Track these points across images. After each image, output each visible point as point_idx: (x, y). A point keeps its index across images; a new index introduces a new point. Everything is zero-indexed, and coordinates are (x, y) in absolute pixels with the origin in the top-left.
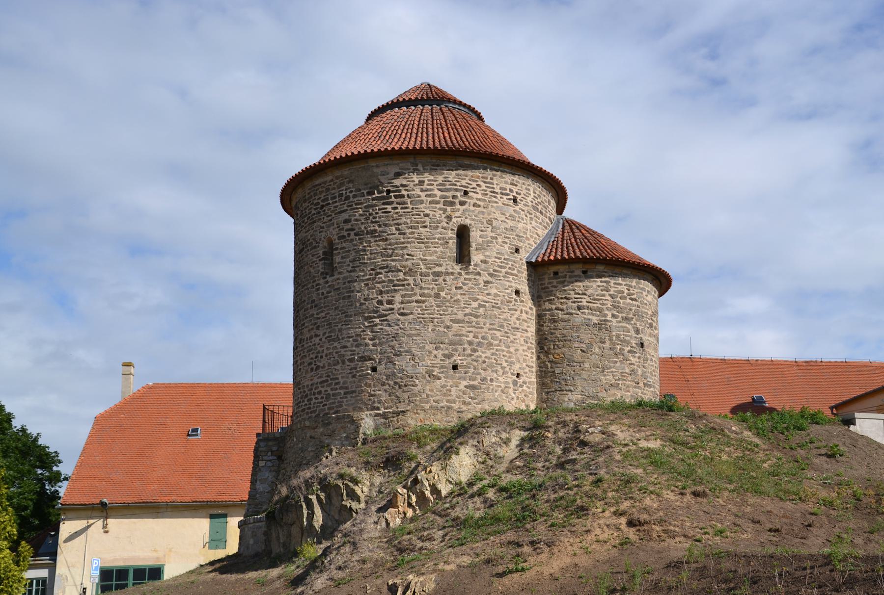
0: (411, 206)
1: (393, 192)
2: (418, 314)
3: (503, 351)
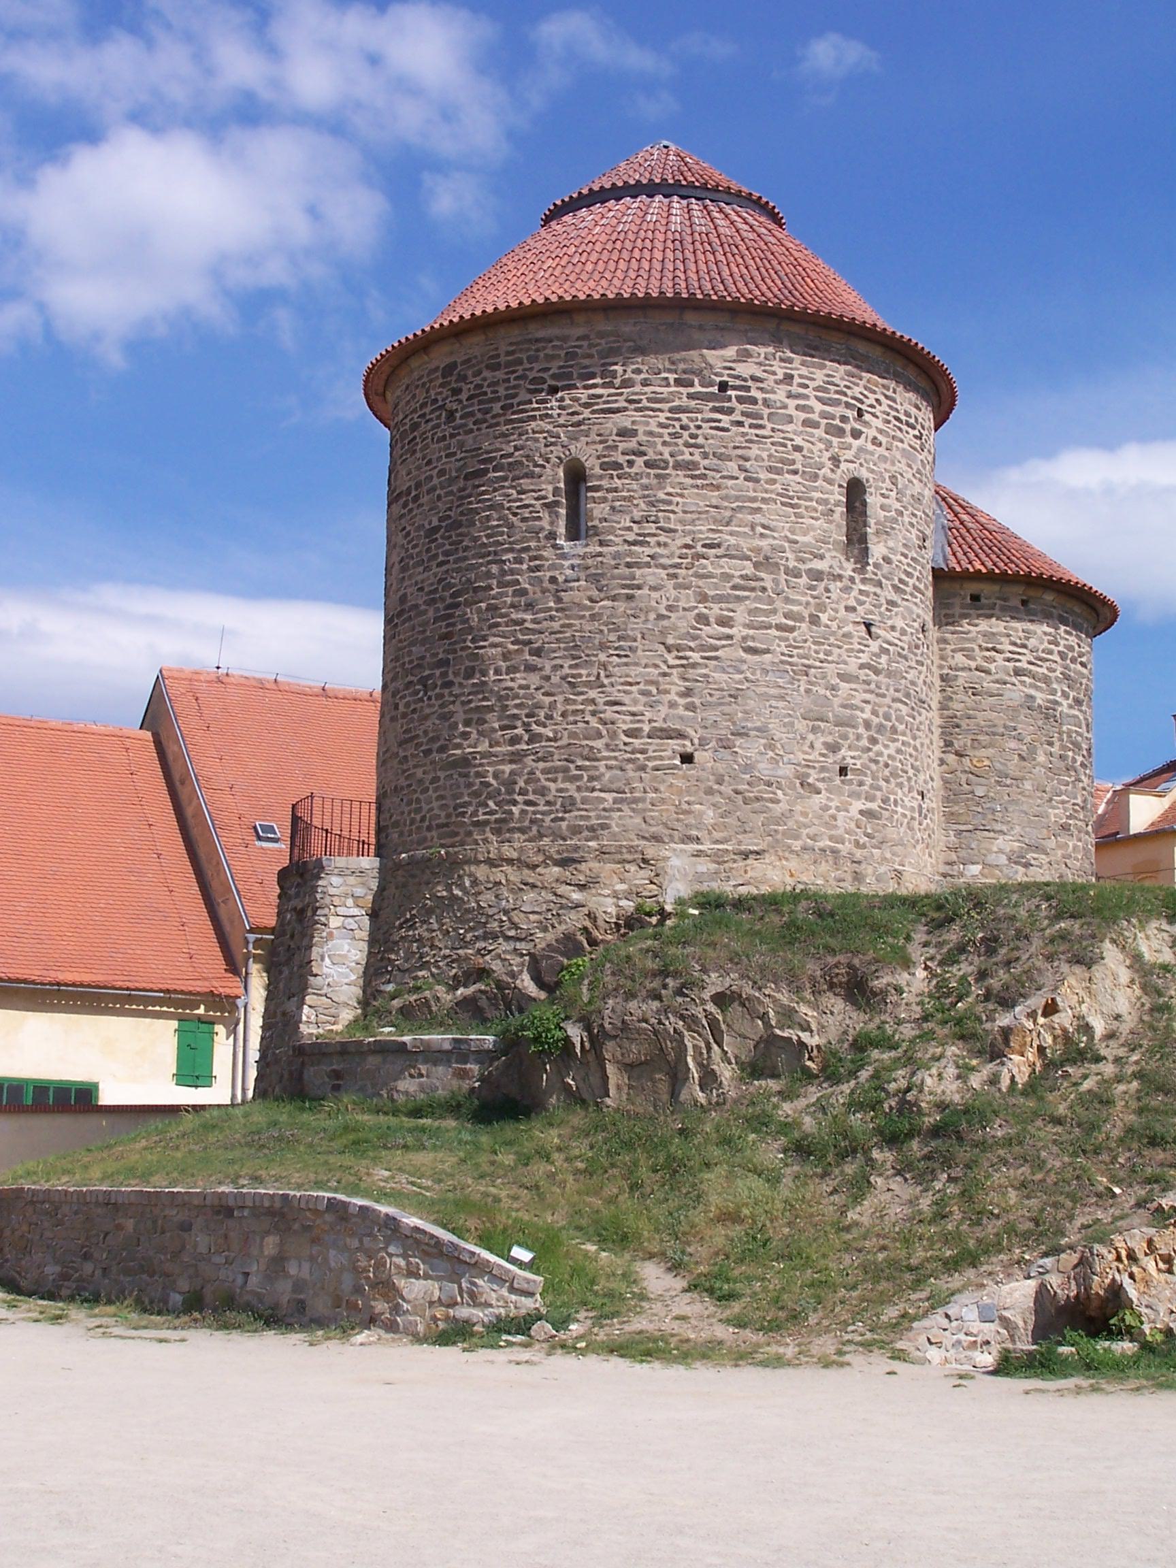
0: (769, 426)
1: (735, 388)
2: (783, 654)
3: (909, 744)
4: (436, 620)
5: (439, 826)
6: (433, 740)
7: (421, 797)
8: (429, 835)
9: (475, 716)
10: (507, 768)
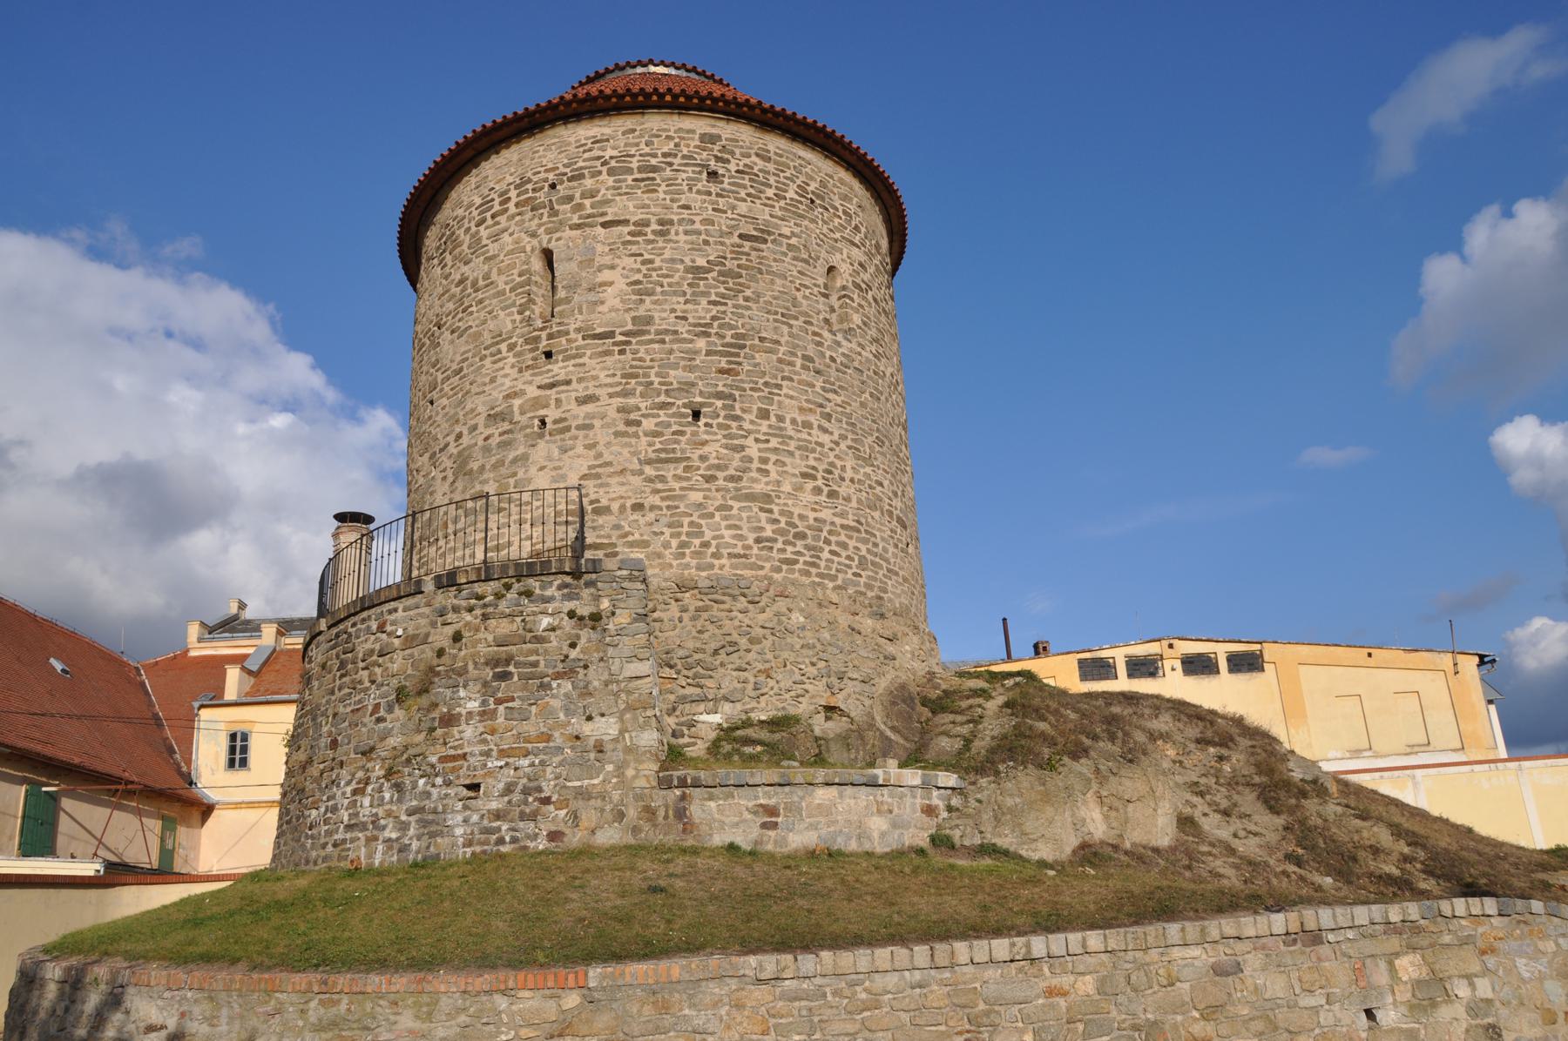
4: (709, 353)
6: (719, 467)
7: (703, 522)
8: (716, 562)
9: (773, 457)
10: (812, 515)
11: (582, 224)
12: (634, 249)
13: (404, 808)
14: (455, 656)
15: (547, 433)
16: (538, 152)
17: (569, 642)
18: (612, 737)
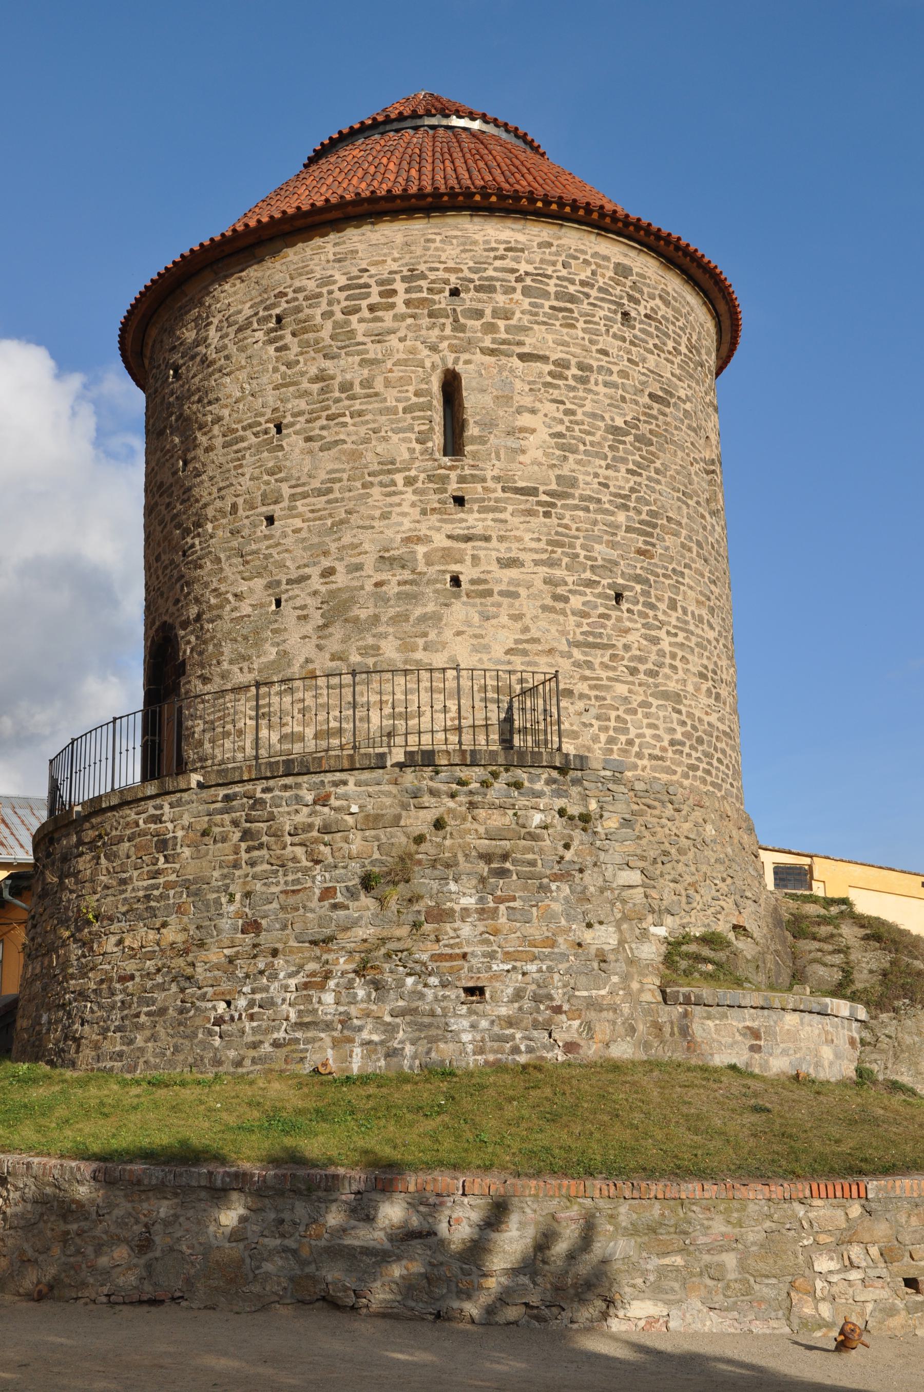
4: (629, 529)
5: (652, 757)
7: (628, 718)
8: (640, 763)
9: (680, 654)
11: (496, 350)
12: (556, 394)
13: (388, 1008)
14: (439, 845)
15: (463, 594)
16: (433, 241)
17: (563, 842)
18: (611, 947)
